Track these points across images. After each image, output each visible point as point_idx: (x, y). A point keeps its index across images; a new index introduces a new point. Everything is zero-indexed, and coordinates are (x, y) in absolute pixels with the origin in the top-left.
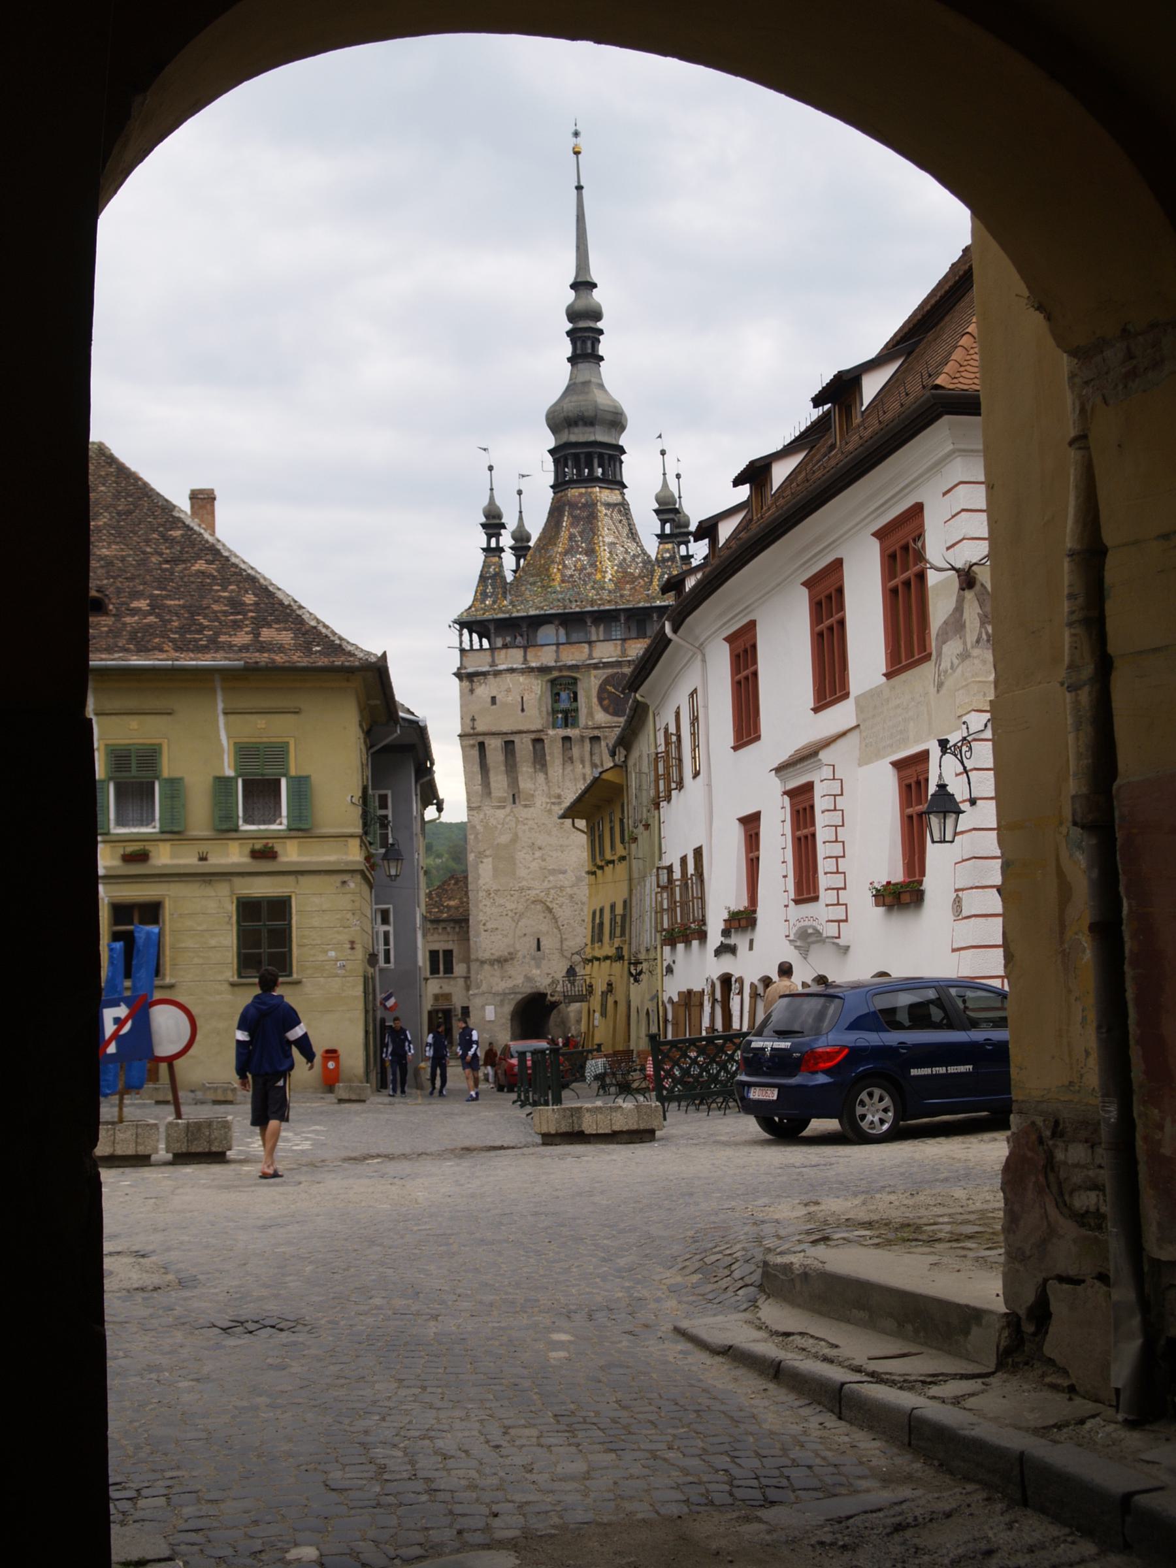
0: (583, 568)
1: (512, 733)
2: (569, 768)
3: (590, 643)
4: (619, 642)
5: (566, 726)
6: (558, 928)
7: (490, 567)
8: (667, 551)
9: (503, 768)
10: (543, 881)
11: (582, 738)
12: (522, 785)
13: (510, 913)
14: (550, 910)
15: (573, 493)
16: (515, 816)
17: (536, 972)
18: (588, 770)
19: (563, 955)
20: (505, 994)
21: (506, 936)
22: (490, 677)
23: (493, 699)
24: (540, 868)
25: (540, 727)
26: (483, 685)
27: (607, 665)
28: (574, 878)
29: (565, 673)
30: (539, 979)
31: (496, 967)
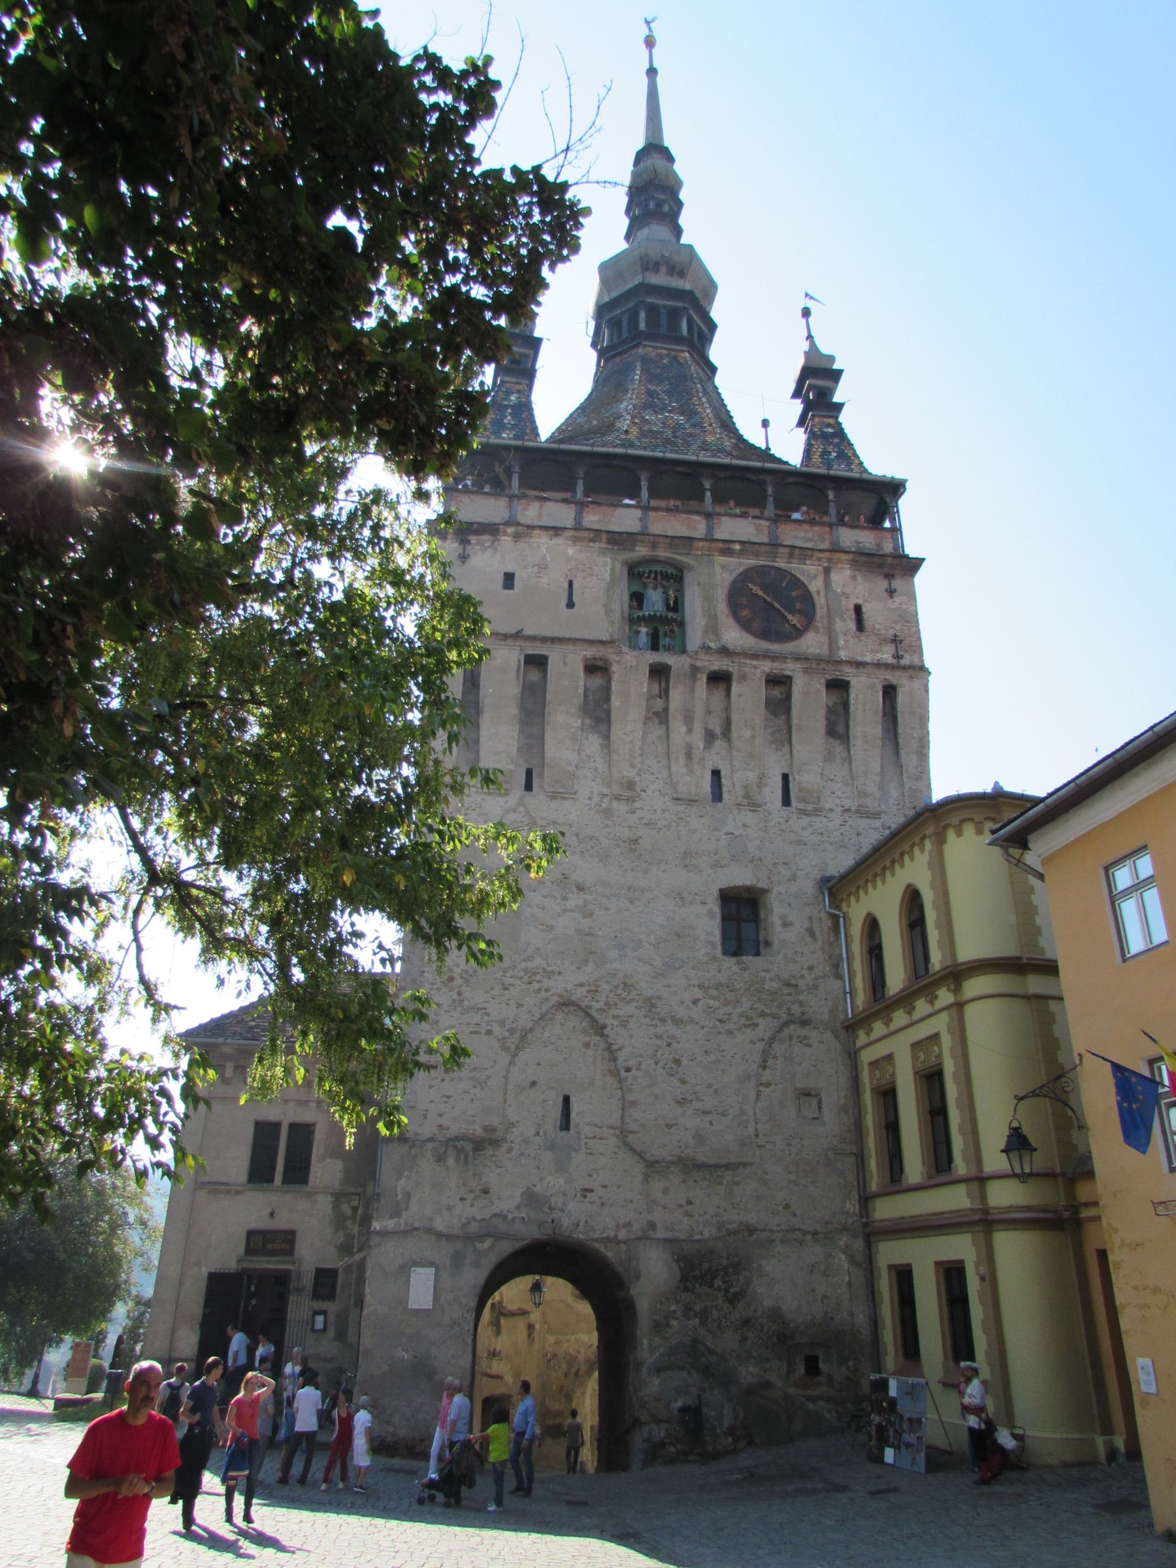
0: (677, 428)
1: (544, 640)
2: (657, 731)
3: (709, 516)
4: (765, 523)
5: (655, 647)
6: (615, 1073)
7: (509, 393)
8: (829, 425)
9: (514, 711)
10: (586, 961)
11: (695, 670)
12: (552, 748)
13: (497, 1030)
14: (600, 1029)
15: (649, 350)
16: (528, 813)
17: (552, 1183)
18: (698, 739)
19: (626, 1144)
20: (469, 1238)
21: (483, 1085)
22: (506, 540)
23: (509, 580)
24: (579, 931)
25: (605, 637)
26: (489, 553)
27: (748, 547)
28: (658, 963)
29: (663, 553)
30: (557, 1201)
31: (451, 1161)
